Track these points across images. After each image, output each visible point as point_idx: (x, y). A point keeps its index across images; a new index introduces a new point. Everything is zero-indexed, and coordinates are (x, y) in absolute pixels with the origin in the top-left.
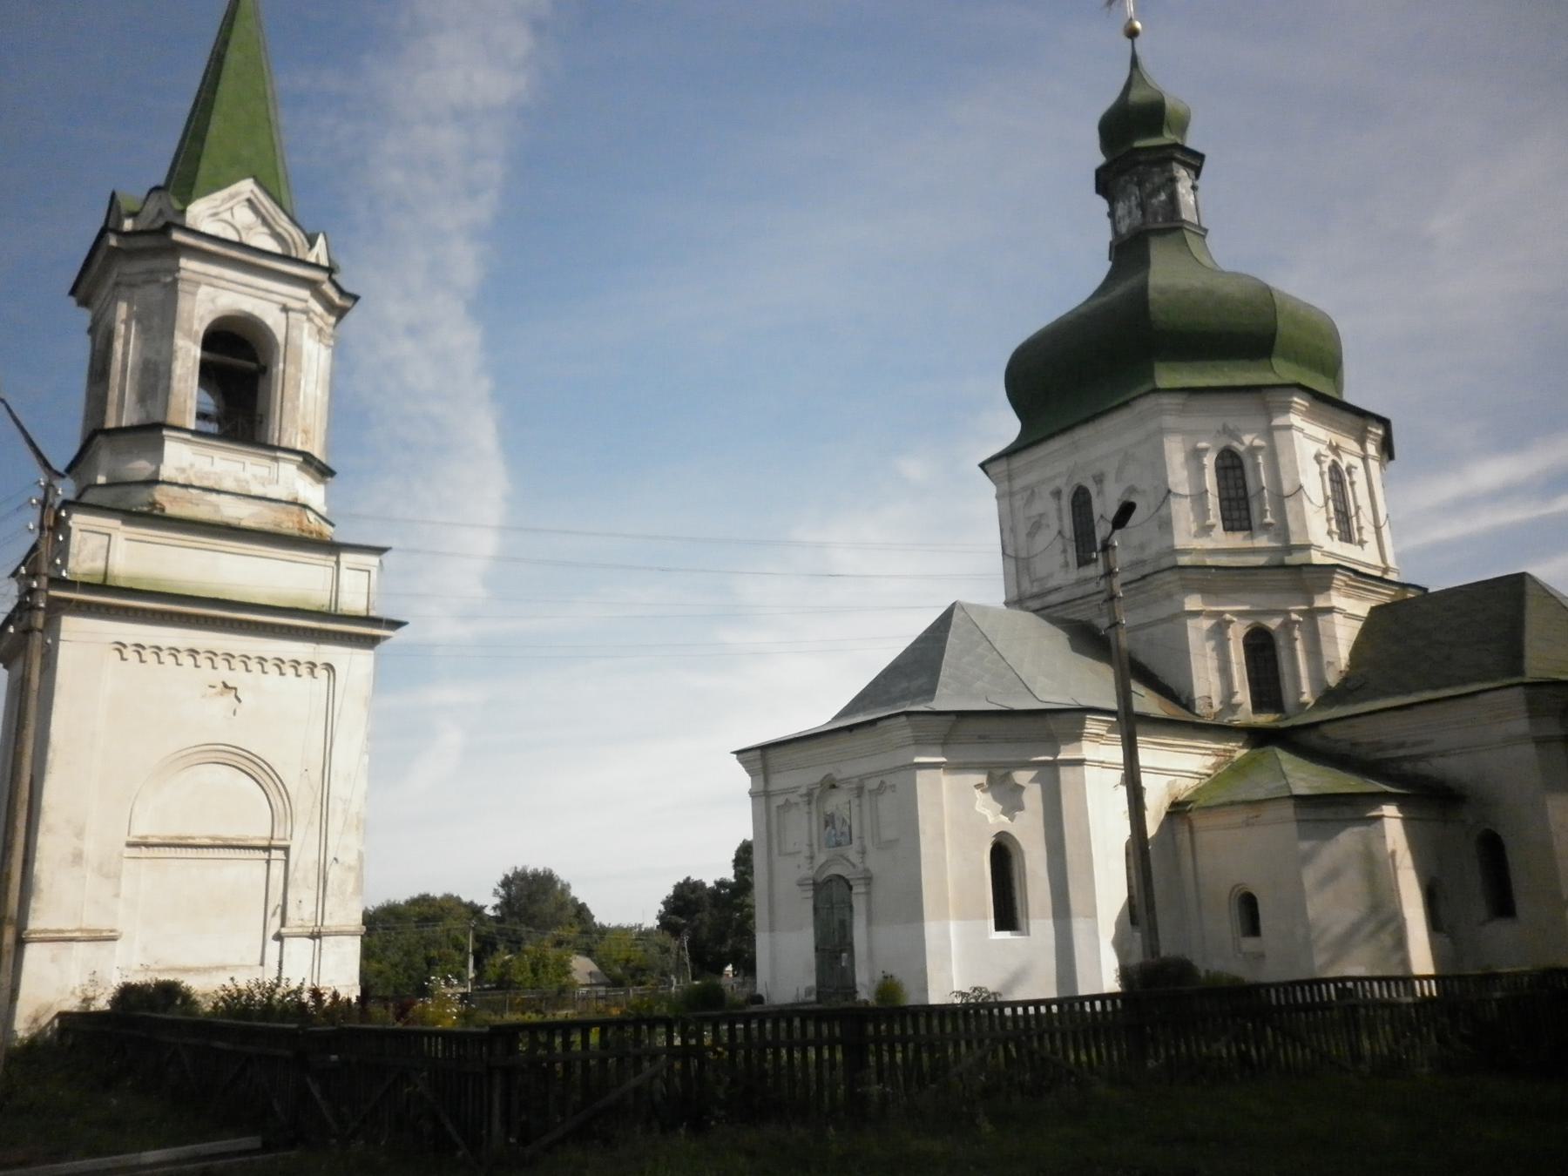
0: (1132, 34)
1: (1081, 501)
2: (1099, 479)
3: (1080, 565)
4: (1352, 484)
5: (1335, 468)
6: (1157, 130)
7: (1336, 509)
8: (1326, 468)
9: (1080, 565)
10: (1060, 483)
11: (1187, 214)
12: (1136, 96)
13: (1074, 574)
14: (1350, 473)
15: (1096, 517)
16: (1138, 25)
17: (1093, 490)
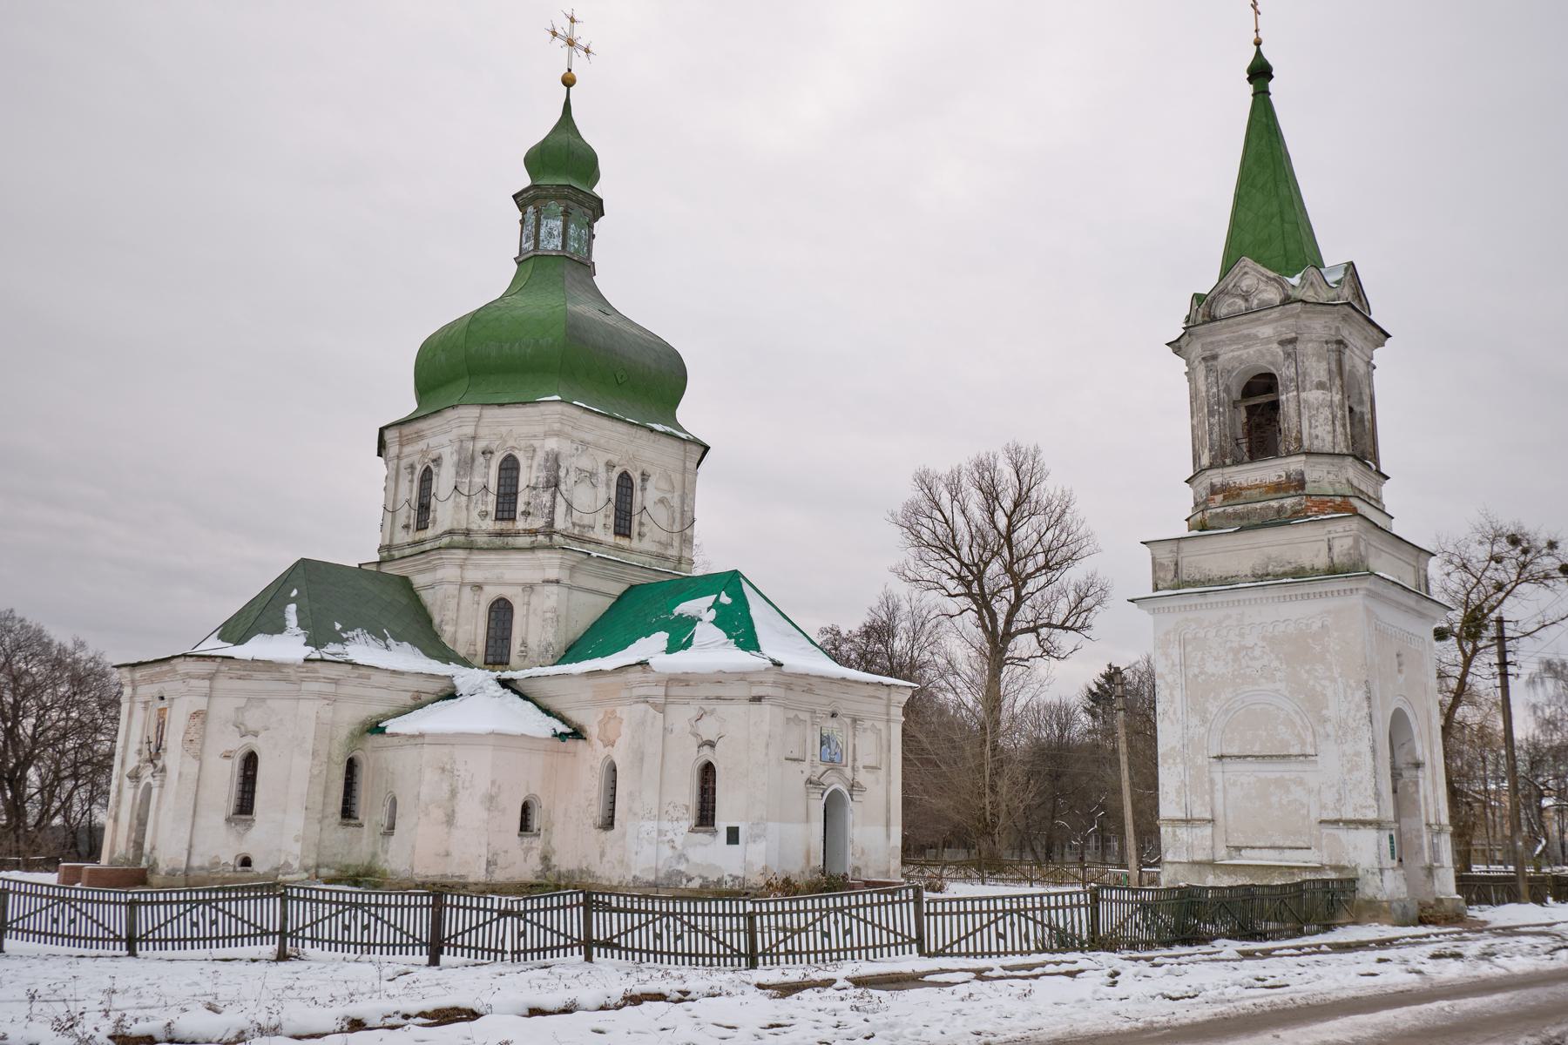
4: (643, 489)
8: (615, 475)
10: (416, 458)
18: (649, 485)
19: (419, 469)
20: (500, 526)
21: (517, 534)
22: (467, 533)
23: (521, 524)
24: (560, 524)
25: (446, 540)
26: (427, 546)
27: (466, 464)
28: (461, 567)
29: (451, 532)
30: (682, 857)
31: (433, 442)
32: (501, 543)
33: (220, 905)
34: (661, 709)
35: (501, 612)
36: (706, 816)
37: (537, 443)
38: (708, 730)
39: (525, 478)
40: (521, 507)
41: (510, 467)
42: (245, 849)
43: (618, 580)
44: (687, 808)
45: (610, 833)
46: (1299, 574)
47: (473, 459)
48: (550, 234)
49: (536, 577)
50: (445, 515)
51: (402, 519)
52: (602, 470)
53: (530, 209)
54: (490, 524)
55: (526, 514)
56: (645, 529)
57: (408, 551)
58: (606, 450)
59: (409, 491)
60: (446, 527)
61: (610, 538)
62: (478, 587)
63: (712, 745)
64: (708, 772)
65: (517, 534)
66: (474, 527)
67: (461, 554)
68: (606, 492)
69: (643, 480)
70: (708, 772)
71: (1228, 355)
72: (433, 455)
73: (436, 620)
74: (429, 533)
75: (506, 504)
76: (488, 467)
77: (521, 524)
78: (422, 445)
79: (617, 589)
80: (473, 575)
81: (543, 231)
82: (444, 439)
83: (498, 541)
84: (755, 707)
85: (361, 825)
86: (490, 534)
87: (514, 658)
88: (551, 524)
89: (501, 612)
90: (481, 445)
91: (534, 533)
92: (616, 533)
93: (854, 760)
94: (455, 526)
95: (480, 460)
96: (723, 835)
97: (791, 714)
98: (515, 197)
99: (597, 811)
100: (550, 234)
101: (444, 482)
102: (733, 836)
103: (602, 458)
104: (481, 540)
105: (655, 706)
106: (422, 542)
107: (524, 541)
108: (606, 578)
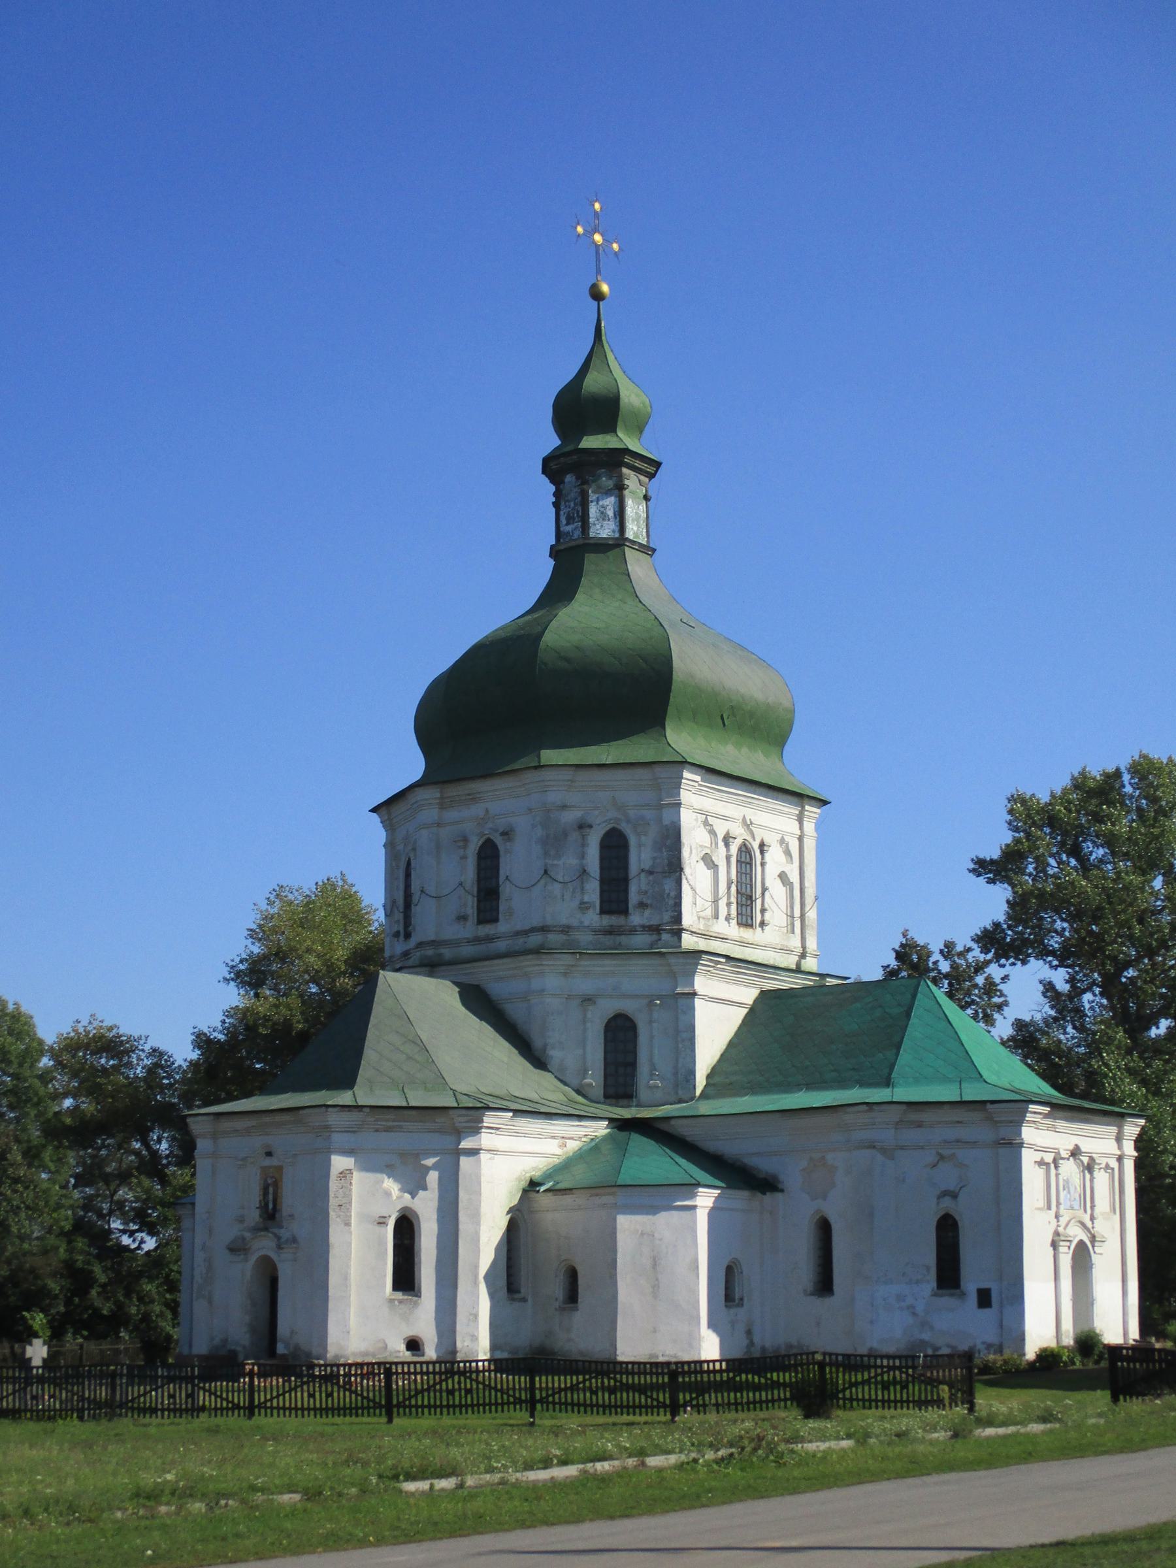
0: (597, 296)
1: (489, 856)
2: (507, 834)
3: (480, 922)
4: (763, 864)
5: (745, 849)
6: (611, 428)
7: (738, 892)
8: (734, 849)
9: (480, 922)
11: (634, 530)
12: (594, 383)
13: (470, 929)
14: (762, 852)
15: (502, 878)
16: (605, 288)
17: (501, 848)
18: (767, 855)
20: (607, 921)
21: (633, 931)
22: (566, 929)
24: (687, 921)
25: (535, 940)
26: (502, 946)
27: (554, 841)
28: (565, 974)
29: (544, 929)
30: (924, 1324)
32: (612, 942)
33: (225, 1404)
34: (888, 1152)
35: (621, 1035)
36: (948, 1275)
37: (648, 814)
38: (947, 1177)
39: (640, 857)
40: (634, 897)
41: (615, 847)
42: (411, 1332)
43: (749, 985)
44: (928, 1269)
45: (828, 1301)
47: (565, 834)
48: (603, 515)
50: (522, 905)
52: (721, 844)
53: (569, 478)
54: (593, 918)
55: (642, 905)
56: (767, 916)
57: (467, 951)
58: (725, 818)
60: (536, 922)
61: (733, 930)
62: (588, 1000)
63: (954, 1196)
64: (947, 1228)
65: (633, 931)
66: (575, 923)
67: (568, 960)
68: (727, 872)
69: (762, 852)
70: (947, 1228)
73: (537, 1043)
74: (502, 927)
75: (614, 896)
76: (584, 845)
77: (636, 919)
78: (477, 810)
79: (749, 995)
80: (585, 986)
81: (593, 510)
83: (608, 940)
84: (1002, 1151)
85: (524, 1300)
86: (596, 932)
87: (643, 1094)
88: (678, 918)
89: (621, 1035)
91: (656, 930)
92: (740, 924)
93: (1092, 1207)
94: (549, 921)
95: (575, 836)
96: (973, 1298)
97: (1038, 1156)
98: (546, 461)
99: (805, 1272)
100: (603, 515)
101: (517, 864)
102: (984, 1299)
103: (721, 829)
104: (585, 938)
105: (884, 1151)
106: (490, 939)
108: (736, 982)
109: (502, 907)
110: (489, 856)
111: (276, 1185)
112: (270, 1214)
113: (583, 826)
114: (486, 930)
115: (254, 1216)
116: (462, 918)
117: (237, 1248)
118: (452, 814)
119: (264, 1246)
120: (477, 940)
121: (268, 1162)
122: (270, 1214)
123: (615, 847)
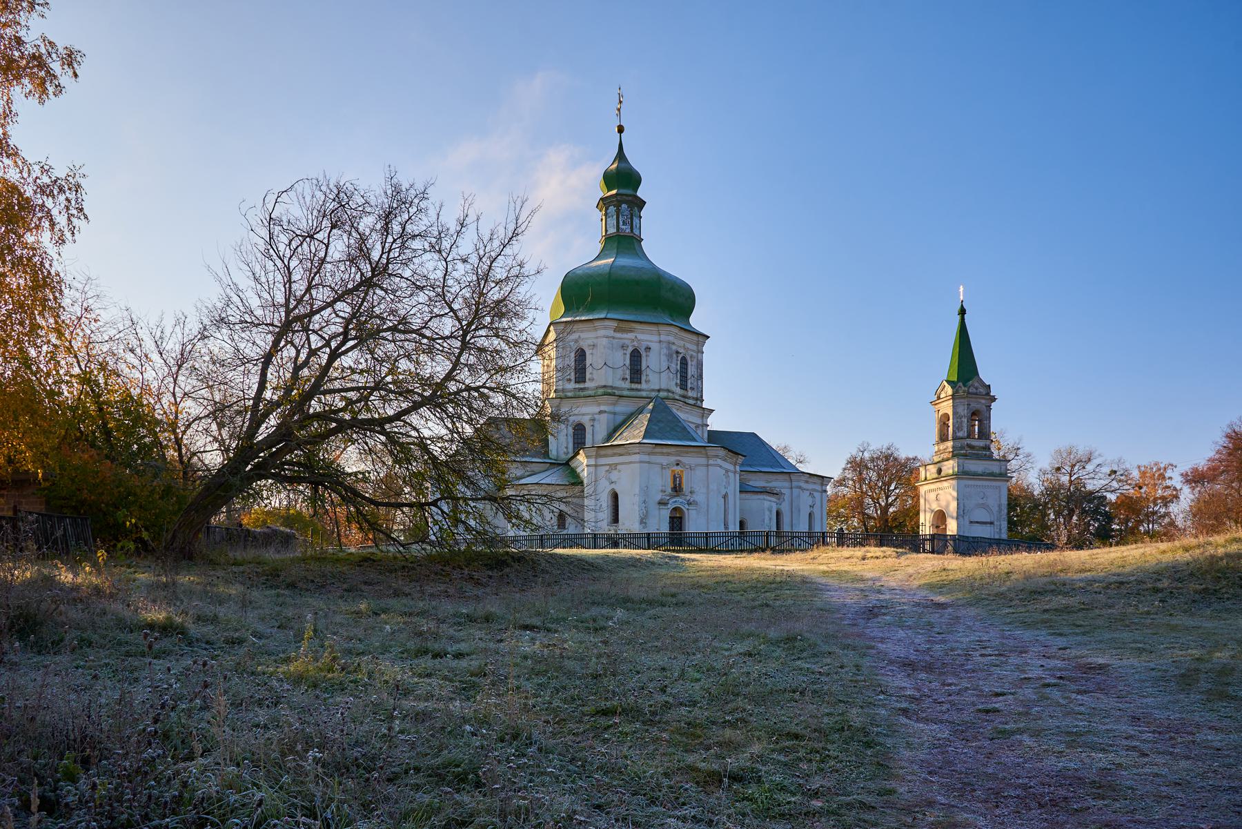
1: (636, 356)
2: (648, 349)
13: (627, 385)
17: (643, 354)
19: (630, 349)
23: (690, 394)
26: (644, 394)
27: (670, 356)
29: (668, 391)
31: (640, 336)
39: (691, 370)
41: (684, 362)
46: (992, 474)
49: (699, 421)
51: (620, 373)
54: (678, 390)
55: (692, 389)
57: (626, 393)
59: (622, 360)
71: (973, 405)
72: (644, 344)
74: (644, 386)
82: (655, 338)
90: (674, 348)
91: (697, 399)
106: (637, 390)
107: (691, 402)
109: (644, 378)
110: (636, 356)
111: (681, 478)
112: (677, 489)
113: (677, 352)
114: (634, 386)
115: (669, 490)
116: (624, 379)
117: (662, 503)
118: (618, 335)
119: (678, 502)
120: (632, 390)
121: (675, 468)
122: (677, 489)
123: (684, 362)
